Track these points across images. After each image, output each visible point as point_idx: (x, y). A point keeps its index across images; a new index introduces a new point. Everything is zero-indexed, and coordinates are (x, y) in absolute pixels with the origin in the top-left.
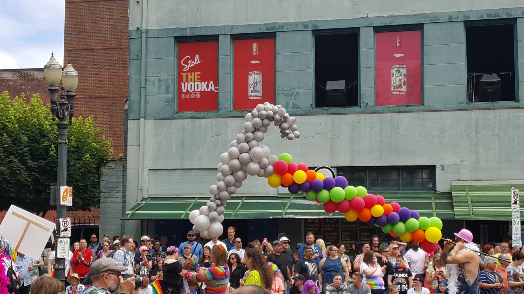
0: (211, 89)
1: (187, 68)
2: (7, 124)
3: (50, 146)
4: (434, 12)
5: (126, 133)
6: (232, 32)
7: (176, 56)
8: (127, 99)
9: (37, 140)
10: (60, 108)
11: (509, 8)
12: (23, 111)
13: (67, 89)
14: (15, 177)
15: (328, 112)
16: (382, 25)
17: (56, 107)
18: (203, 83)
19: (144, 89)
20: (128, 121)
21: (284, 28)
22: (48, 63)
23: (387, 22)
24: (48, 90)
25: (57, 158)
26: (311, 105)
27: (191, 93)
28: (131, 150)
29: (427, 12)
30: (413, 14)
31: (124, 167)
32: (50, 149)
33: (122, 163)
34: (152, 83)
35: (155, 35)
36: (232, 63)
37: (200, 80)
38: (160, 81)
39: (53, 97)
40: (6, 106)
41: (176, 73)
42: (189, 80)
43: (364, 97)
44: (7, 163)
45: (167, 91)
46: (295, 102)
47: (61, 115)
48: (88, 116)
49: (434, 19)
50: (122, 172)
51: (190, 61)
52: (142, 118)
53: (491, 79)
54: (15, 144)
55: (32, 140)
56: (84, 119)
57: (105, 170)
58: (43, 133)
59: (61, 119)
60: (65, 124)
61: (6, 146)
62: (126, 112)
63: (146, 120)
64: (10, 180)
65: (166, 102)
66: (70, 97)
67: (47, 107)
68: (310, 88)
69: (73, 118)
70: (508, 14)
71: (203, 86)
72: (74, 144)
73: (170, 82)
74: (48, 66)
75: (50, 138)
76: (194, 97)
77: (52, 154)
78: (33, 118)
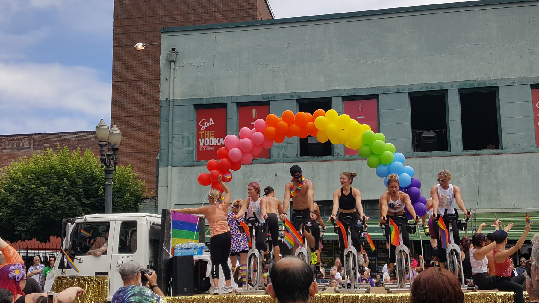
0: (222, 144)
1: (204, 128)
2: (66, 171)
3: (99, 187)
4: (386, 85)
5: (157, 177)
6: (237, 101)
7: (195, 119)
8: (158, 152)
9: (90, 183)
10: (107, 158)
11: (442, 82)
12: (79, 161)
13: (112, 143)
14: (73, 211)
15: (310, 159)
16: (348, 95)
17: (104, 158)
18: (215, 139)
19: (171, 144)
20: (159, 168)
21: (276, 98)
22: (98, 124)
23: (352, 93)
24: (99, 145)
25: (105, 197)
26: (297, 154)
27: (206, 147)
28: (161, 190)
29: (381, 86)
30: (371, 87)
31: (156, 203)
32: (99, 190)
33: (154, 200)
34: (177, 139)
35: (179, 103)
36: (237, 124)
37: (213, 137)
38: (183, 137)
39: (102, 150)
40: (66, 157)
41: (195, 131)
42: (205, 137)
43: (336, 148)
44: (66, 201)
45: (189, 145)
46: (285, 152)
47: (108, 163)
48: (129, 164)
49: (386, 90)
50: (154, 207)
51: (206, 123)
52: (170, 165)
53: (429, 135)
54: (73, 186)
55: (86, 183)
56: (125, 167)
57: (141, 205)
58: (94, 178)
59: (108, 167)
60: (109, 170)
61: (65, 188)
62: (158, 161)
63: (173, 168)
64: (68, 214)
65: (188, 154)
66: (115, 150)
67: (98, 158)
68: (296, 142)
69: (117, 166)
70: (441, 87)
71: (216, 141)
72: (117, 185)
73: (191, 138)
74: (99, 126)
75: (99, 182)
76: (209, 149)
77: (101, 194)
78: (86, 166)
